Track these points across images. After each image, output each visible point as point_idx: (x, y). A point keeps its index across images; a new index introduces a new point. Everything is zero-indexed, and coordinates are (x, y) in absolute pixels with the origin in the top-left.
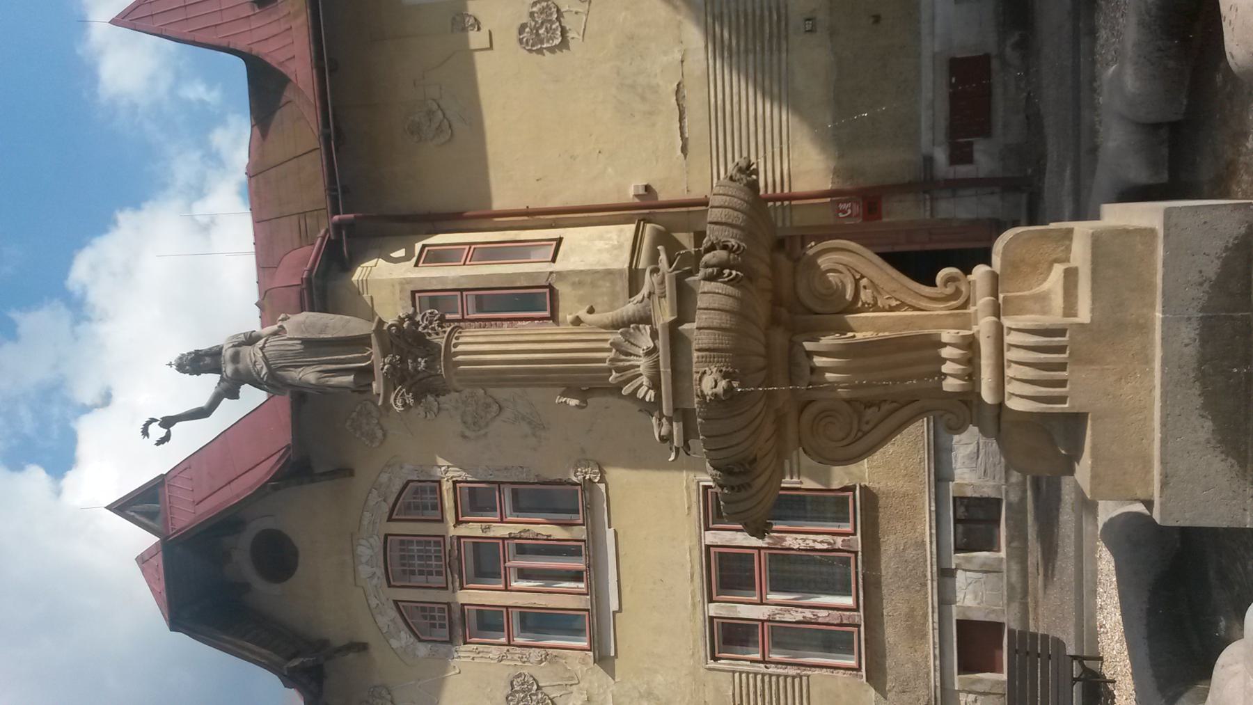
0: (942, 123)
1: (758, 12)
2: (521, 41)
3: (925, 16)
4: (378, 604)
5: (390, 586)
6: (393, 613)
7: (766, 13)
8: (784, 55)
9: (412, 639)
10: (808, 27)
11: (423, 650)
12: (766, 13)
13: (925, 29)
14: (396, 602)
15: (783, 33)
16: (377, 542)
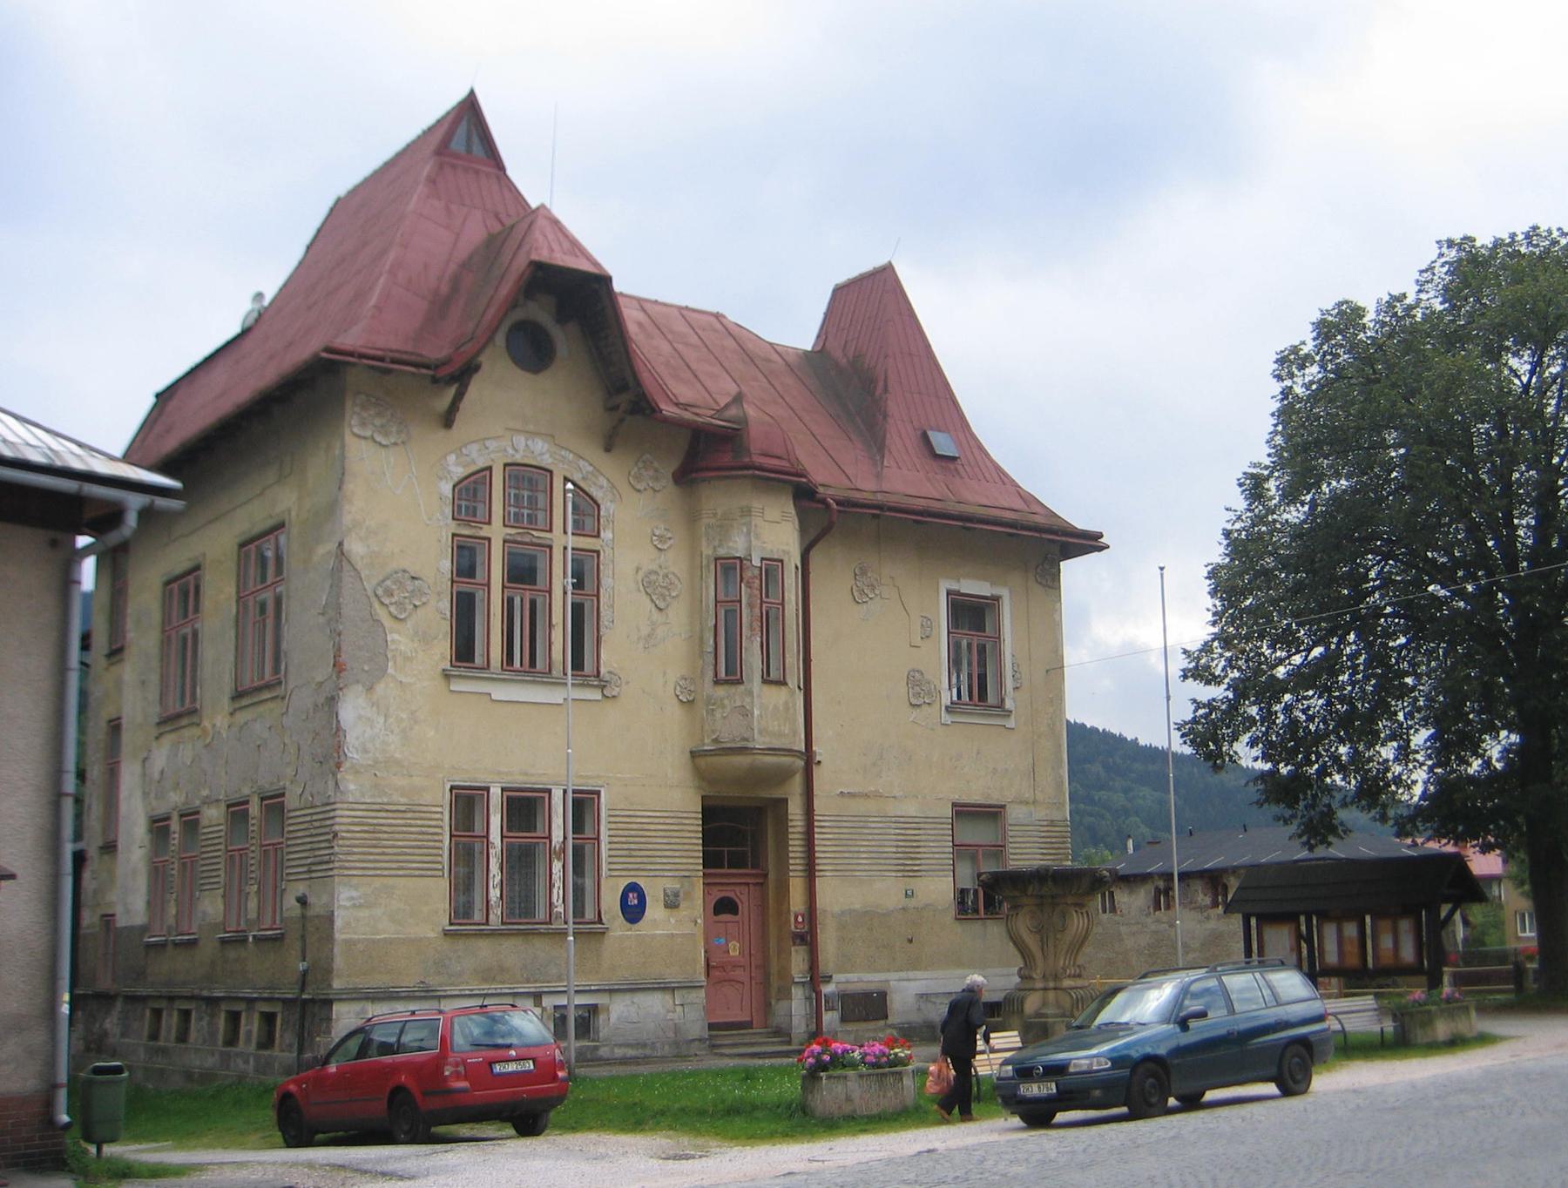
0: (851, 988)
1: (919, 856)
2: (914, 671)
3: (911, 974)
4: (487, 448)
5: (506, 465)
6: (481, 464)
7: (918, 862)
8: (894, 874)
9: (456, 479)
10: (909, 893)
11: (446, 488)
12: (918, 862)
13: (903, 975)
14: (490, 469)
15: (906, 874)
16: (546, 461)
